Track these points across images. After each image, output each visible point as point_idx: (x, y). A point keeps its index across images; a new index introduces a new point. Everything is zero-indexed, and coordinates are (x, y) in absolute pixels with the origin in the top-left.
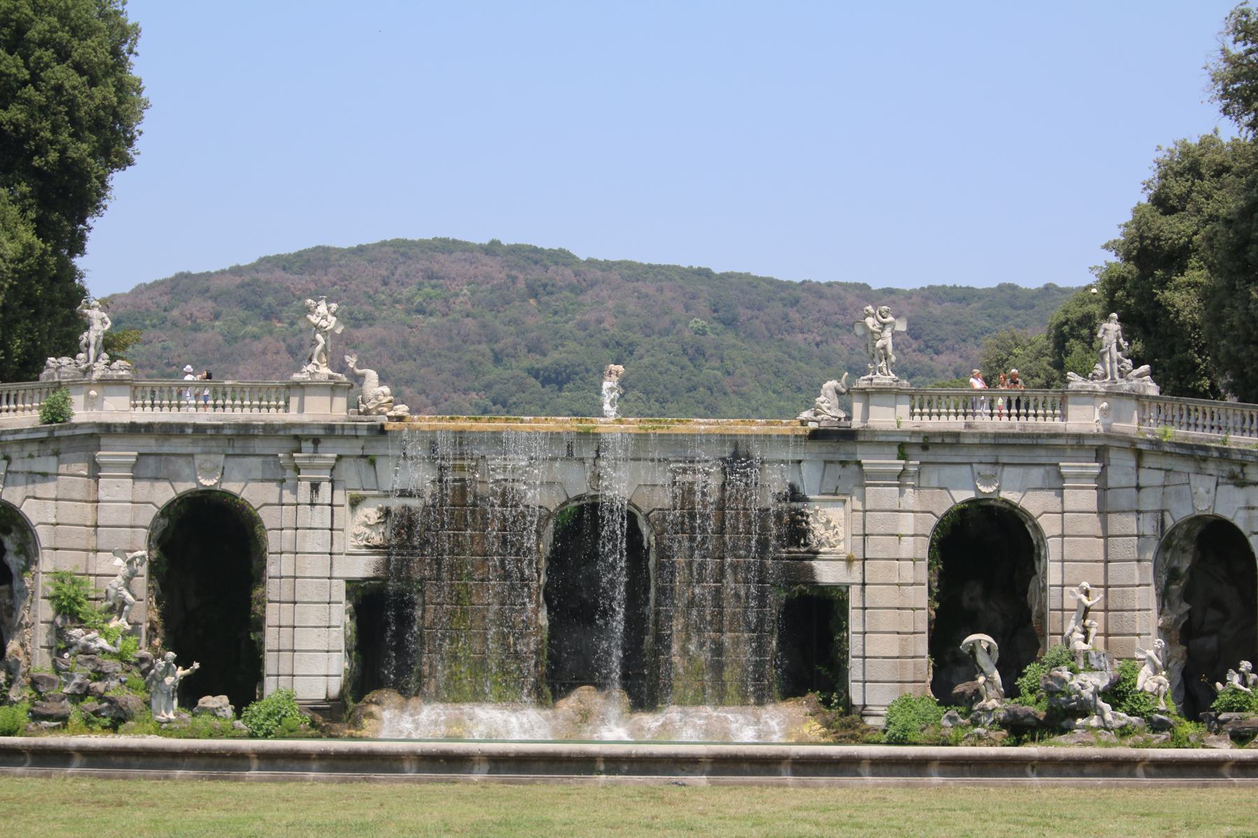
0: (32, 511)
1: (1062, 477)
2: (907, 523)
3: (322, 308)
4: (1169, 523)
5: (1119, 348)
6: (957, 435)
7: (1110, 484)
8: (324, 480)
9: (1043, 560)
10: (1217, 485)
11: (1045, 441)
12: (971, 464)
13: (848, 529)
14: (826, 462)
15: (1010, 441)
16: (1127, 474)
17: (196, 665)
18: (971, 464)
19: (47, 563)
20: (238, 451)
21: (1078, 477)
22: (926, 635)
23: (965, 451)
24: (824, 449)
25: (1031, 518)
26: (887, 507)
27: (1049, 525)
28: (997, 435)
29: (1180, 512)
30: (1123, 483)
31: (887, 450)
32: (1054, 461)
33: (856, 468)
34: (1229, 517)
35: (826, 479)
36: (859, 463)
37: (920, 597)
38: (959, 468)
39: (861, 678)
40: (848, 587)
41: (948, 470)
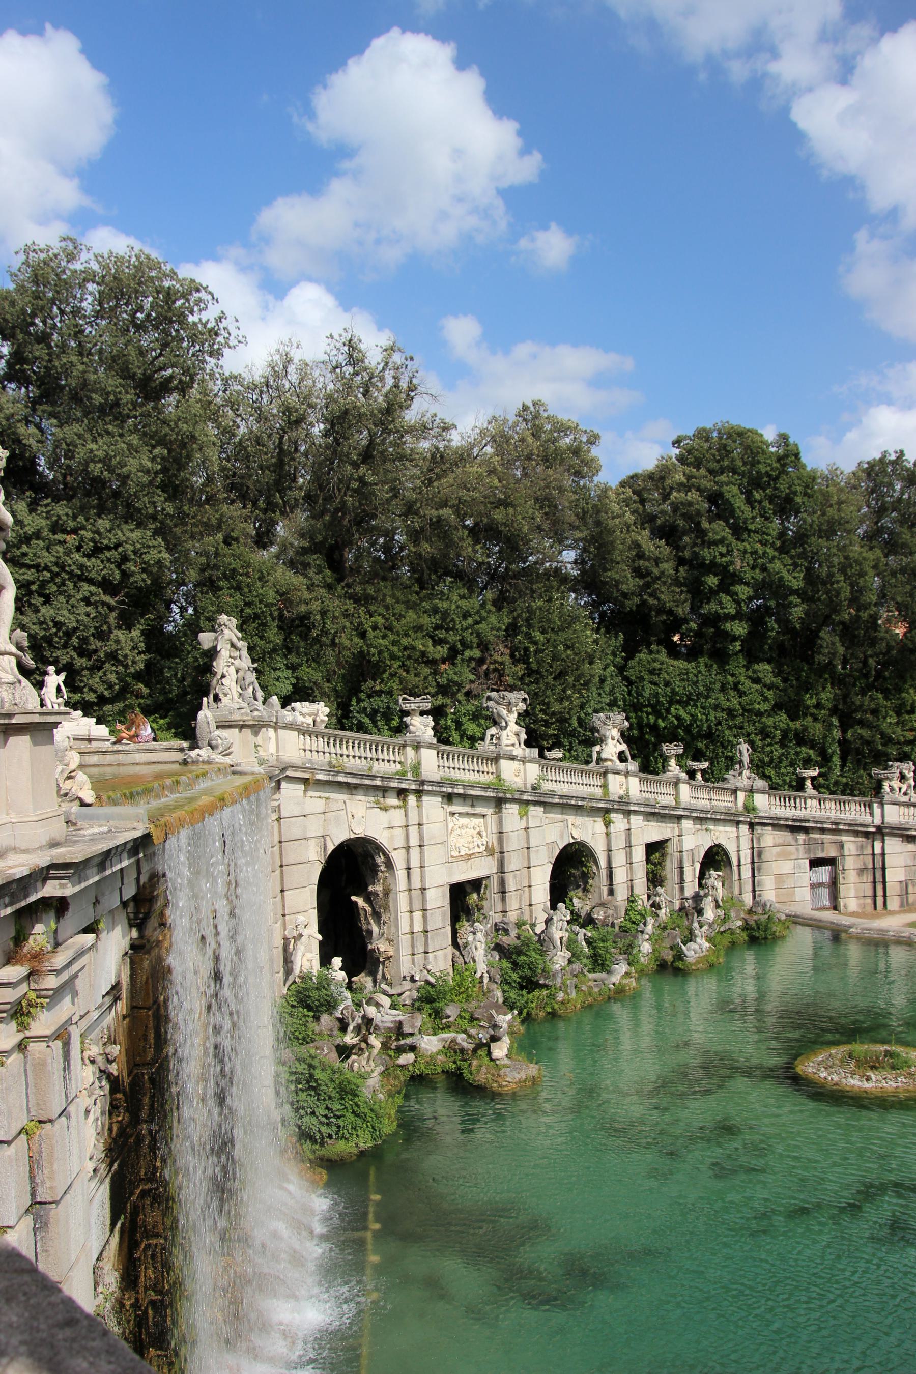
4: (330, 848)
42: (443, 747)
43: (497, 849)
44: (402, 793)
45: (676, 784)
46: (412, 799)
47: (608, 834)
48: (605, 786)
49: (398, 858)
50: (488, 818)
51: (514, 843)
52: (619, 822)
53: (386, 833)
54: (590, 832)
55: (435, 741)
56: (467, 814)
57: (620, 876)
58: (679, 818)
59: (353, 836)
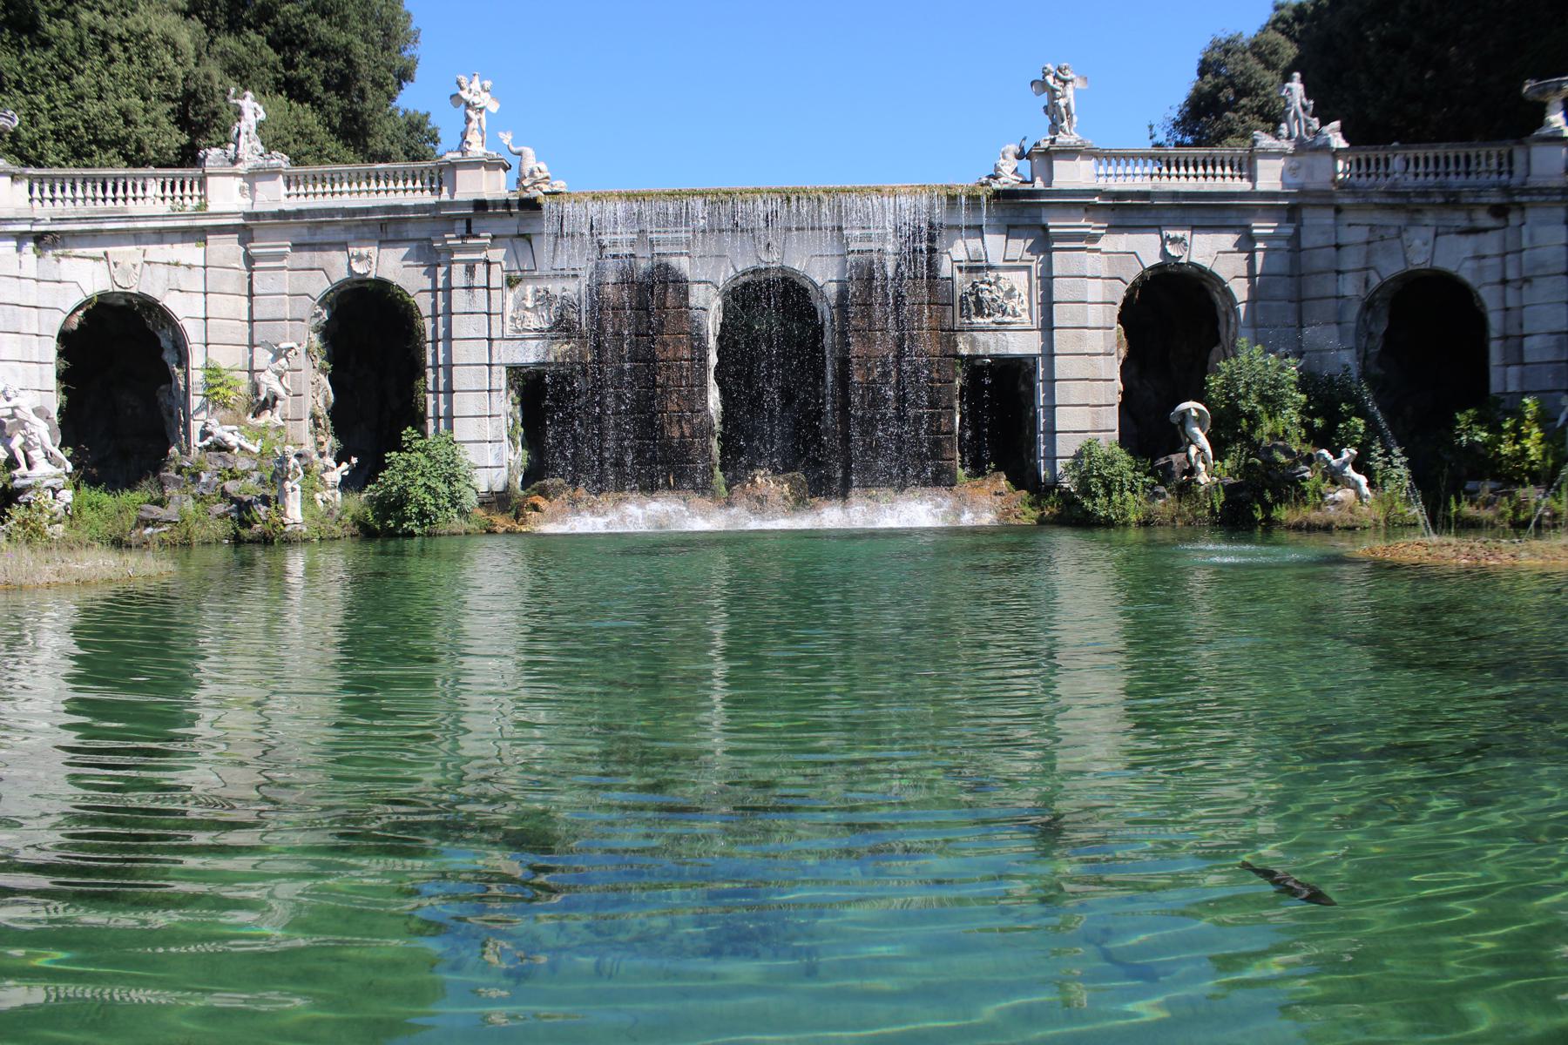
0: (175, 304)
2: (1095, 290)
3: (476, 85)
4: (1375, 281)
5: (1305, 108)
6: (1145, 195)
7: (1305, 244)
8: (478, 261)
10: (1436, 235)
16: (1324, 233)
17: (354, 460)
19: (197, 359)
20: (390, 236)
23: (1154, 212)
24: (1008, 213)
25: (1221, 282)
29: (1391, 267)
30: (1320, 243)
31: (1073, 212)
33: (1040, 232)
34: (1452, 268)
36: (1045, 228)
37: (1112, 368)
46: (1514, 219)
49: (1489, 298)
53: (1468, 264)
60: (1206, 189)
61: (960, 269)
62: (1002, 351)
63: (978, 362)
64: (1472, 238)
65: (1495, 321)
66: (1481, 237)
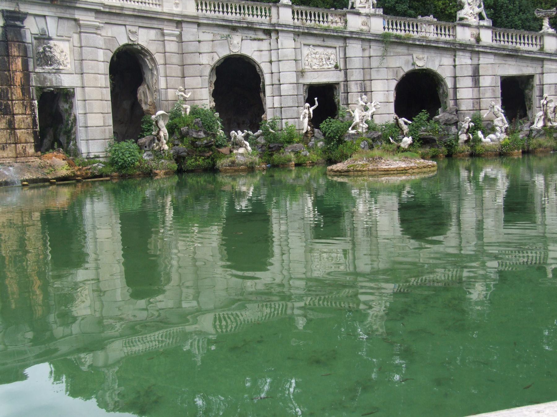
1: (163, 35)
7: (184, 39)
9: (155, 78)
10: (242, 40)
11: (158, 16)
12: (125, 25)
13: (72, 57)
14: (60, 18)
15: (145, 15)
16: (193, 35)
18: (125, 25)
21: (170, 35)
22: (111, 114)
23: (123, 18)
26: (92, 45)
27: (159, 59)
28: (139, 11)
32: (160, 27)
35: (59, 28)
38: (120, 27)
39: (85, 138)
40: (74, 89)
41: (115, 28)
42: (296, 7)
43: (342, 66)
44: (268, 32)
45: (542, 37)
46: (274, 36)
47: (455, 66)
48: (455, 36)
49: (265, 68)
50: (338, 49)
51: (356, 63)
52: (464, 59)
53: (256, 53)
54: (437, 63)
55: (290, 3)
56: (319, 46)
57: (466, 93)
58: (542, 60)
59: (232, 53)
60: (143, 8)
61: (35, 38)
62: (59, 84)
63: (45, 90)
64: (256, 43)
65: (267, 79)
66: (260, 42)
